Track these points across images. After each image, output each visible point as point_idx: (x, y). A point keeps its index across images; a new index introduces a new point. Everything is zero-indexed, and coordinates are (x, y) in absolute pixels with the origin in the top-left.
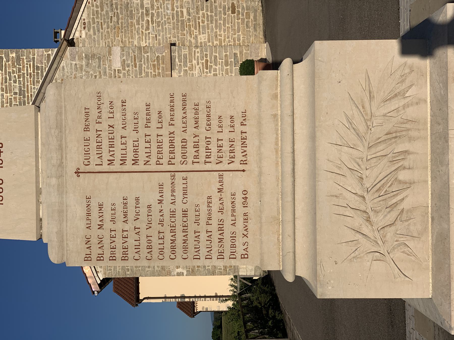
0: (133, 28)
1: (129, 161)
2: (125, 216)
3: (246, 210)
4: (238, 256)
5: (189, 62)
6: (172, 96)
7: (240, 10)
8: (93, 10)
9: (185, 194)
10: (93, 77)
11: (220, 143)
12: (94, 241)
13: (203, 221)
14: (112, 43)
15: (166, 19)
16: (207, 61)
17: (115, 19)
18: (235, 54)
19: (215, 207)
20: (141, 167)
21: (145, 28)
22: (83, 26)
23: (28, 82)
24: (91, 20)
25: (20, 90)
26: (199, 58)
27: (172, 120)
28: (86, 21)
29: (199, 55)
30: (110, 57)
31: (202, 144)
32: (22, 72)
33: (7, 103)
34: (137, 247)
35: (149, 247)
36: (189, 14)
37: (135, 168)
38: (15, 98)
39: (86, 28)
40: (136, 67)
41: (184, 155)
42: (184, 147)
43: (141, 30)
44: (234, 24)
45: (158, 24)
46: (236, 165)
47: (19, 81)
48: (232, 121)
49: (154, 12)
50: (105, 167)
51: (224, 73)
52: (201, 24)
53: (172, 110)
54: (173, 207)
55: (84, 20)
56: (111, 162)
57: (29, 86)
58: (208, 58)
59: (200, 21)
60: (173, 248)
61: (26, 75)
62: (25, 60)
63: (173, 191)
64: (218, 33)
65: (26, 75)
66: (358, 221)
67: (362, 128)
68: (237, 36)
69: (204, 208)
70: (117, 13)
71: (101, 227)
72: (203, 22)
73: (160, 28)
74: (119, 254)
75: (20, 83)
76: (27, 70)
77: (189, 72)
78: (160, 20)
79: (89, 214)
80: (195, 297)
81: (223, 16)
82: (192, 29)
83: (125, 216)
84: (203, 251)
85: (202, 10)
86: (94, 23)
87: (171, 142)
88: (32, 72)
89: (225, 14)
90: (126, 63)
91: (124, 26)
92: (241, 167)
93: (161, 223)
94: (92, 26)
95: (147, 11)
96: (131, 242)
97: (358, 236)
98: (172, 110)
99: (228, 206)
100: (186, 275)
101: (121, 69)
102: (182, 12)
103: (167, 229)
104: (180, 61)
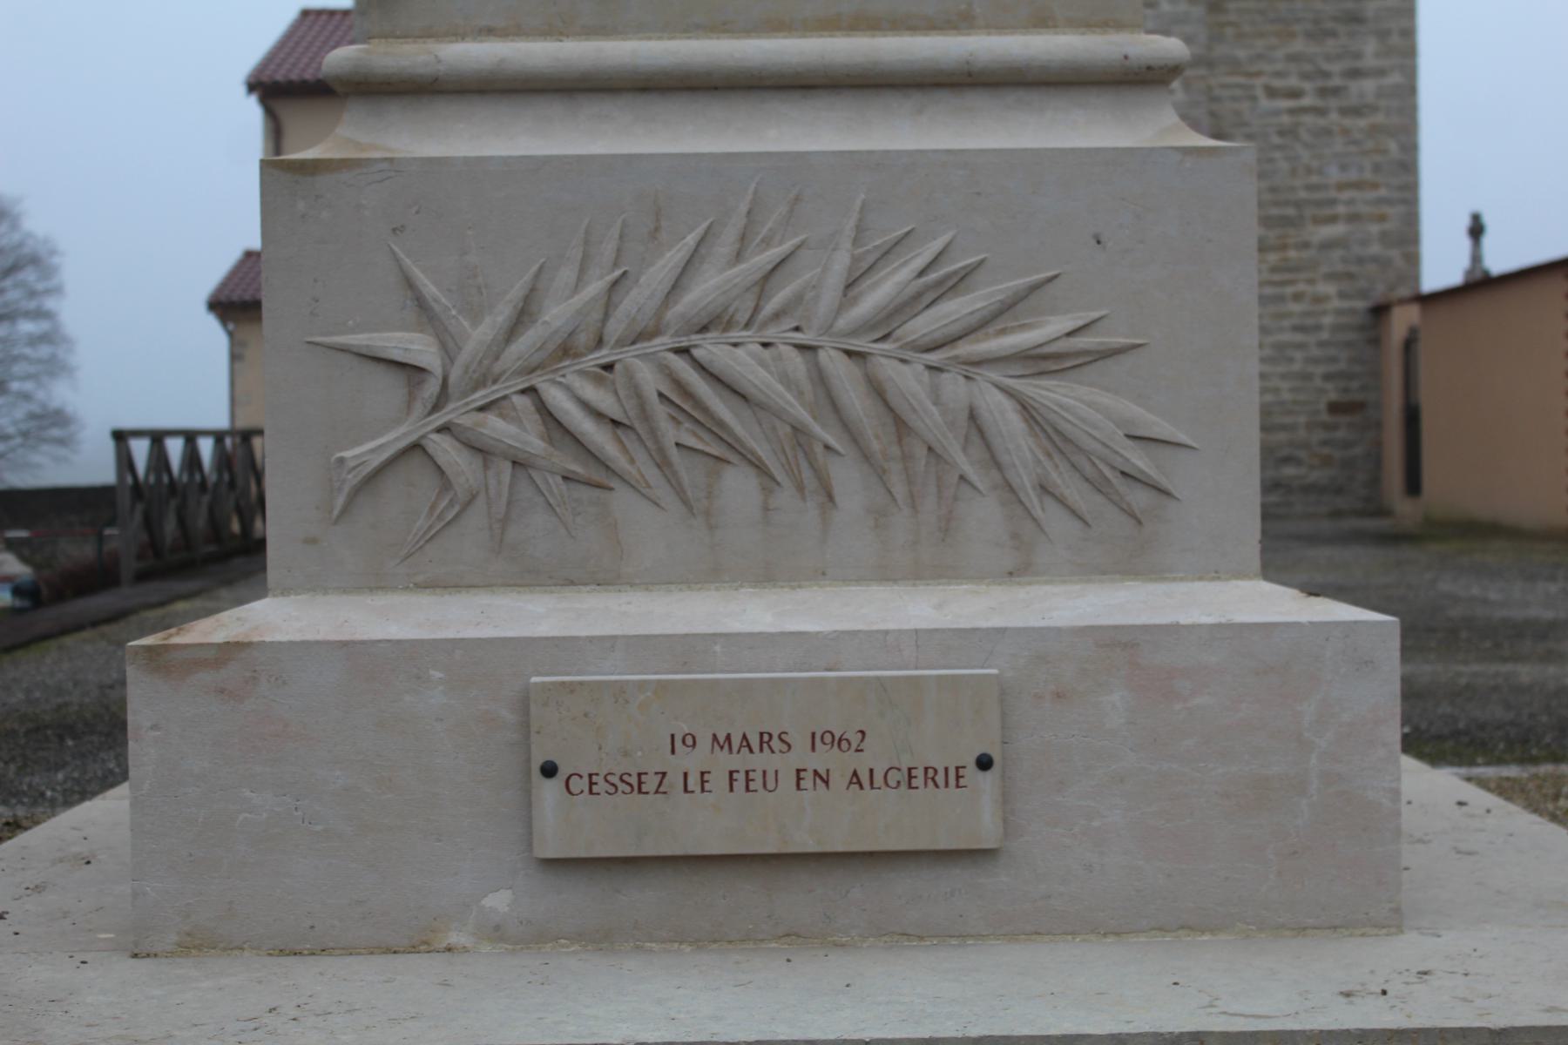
21: (1277, 83)
36: (1327, 245)
52: (1289, 290)
59: (1301, 287)
66: (556, 315)
67: (924, 325)
72: (1297, 297)
73: (1276, 140)
78: (1305, 136)
85: (1342, 295)
89: (1328, 377)
95: (1336, 92)
97: (502, 314)
102: (1333, 219)
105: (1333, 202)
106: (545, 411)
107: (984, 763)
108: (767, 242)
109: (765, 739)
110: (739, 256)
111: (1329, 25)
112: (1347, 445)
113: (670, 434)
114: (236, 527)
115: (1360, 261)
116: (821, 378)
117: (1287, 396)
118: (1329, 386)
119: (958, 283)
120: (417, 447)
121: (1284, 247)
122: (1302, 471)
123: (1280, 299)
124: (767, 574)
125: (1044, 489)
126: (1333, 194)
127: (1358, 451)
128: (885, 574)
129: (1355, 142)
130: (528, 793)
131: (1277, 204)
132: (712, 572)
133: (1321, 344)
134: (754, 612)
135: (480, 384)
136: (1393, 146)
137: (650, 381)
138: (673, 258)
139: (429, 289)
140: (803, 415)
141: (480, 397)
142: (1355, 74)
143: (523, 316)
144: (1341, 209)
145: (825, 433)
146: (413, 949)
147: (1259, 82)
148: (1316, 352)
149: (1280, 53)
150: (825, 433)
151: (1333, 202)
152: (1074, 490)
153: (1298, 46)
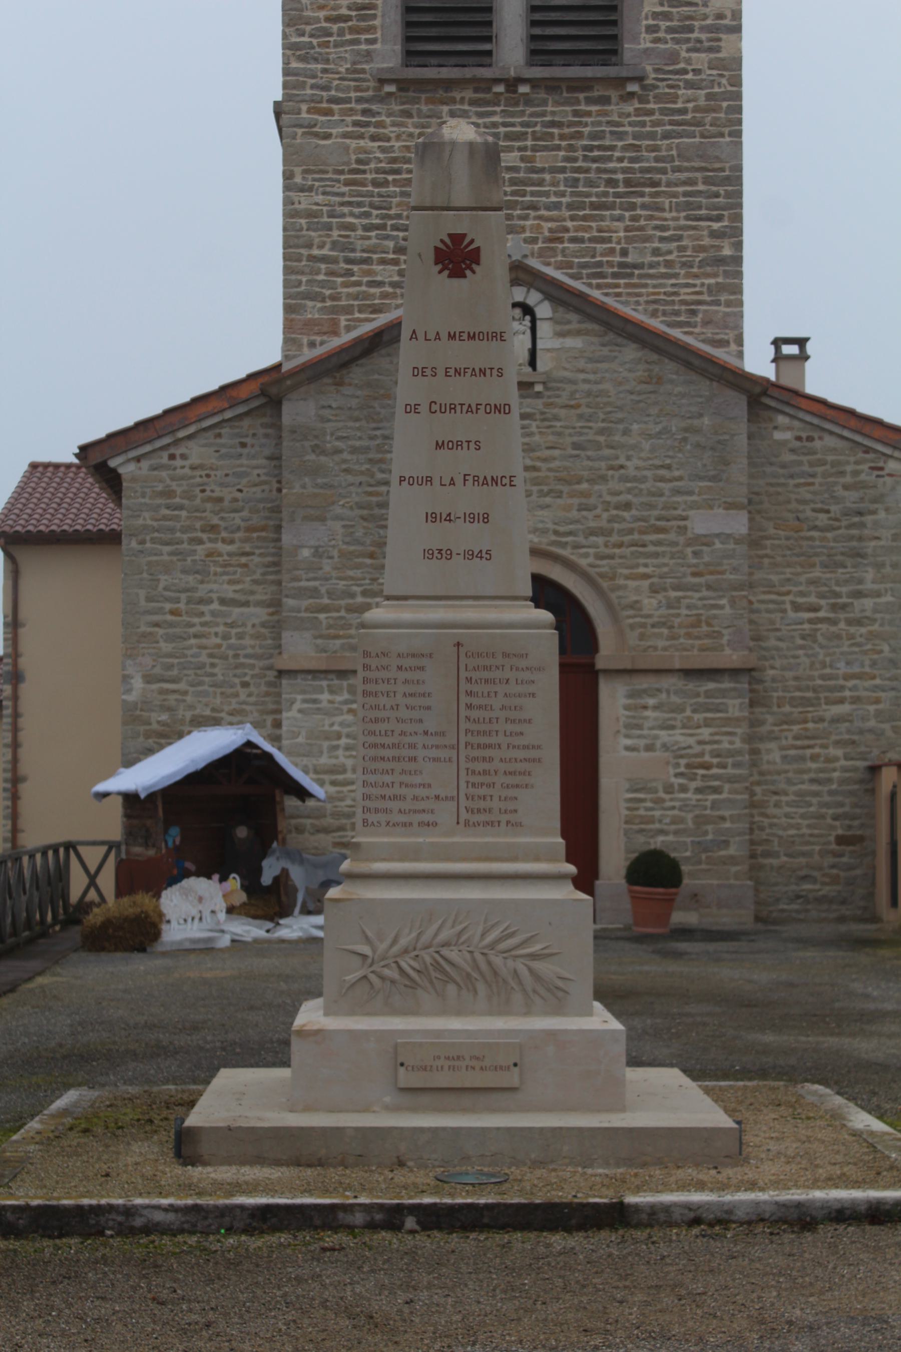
0: (799, 570)
1: (469, 700)
2: (411, 695)
3: (415, 824)
4: (366, 816)
5: (705, 719)
6: (539, 747)
7: (845, 859)
8: (848, 463)
9: (434, 760)
10: (668, 461)
11: (488, 798)
12: (385, 661)
13: (406, 778)
14: (759, 512)
15: (821, 657)
16: (707, 767)
17: (822, 519)
18: (726, 844)
19: (421, 792)
20: (463, 713)
21: (800, 600)
22: (804, 435)
23: (655, 286)
24: (819, 456)
25: (635, 266)
26: (715, 746)
27: (514, 747)
28: (818, 444)
29: (726, 745)
30: (719, 506)
31: (487, 779)
32: (683, 272)
33: (600, 230)
34: (377, 707)
35: (377, 720)
36: (836, 720)
37: (462, 706)
38: (612, 251)
39: (798, 444)
40: (695, 574)
41: (475, 759)
42: (484, 759)
43: (794, 589)
44: (808, 843)
45: (809, 635)
46: (464, 815)
47: (658, 264)
48: (511, 812)
49: (842, 625)
50: (463, 674)
51: (676, 812)
52: (808, 752)
53: (526, 747)
54: (420, 746)
55: (821, 438)
56: (469, 680)
57: (643, 290)
58: (715, 771)
59: (817, 750)
60: (375, 746)
61: (673, 281)
62: (712, 281)
63: (437, 747)
64: (784, 799)
65: (673, 281)
66: (403, 942)
67: (503, 946)
68: (776, 848)
69: (418, 780)
70: (839, 528)
71: (400, 668)
73: (800, 642)
74: (370, 687)
75: (651, 266)
76: (687, 285)
77: (680, 717)
78: (820, 639)
79: (413, 656)
80: (16, 715)
81: (831, 811)
82: (796, 728)
83: (411, 695)
84: (372, 778)
86: (811, 464)
87: (490, 746)
88: (682, 297)
89: (836, 818)
90: (705, 548)
91: (805, 543)
92: (462, 821)
93: (403, 733)
94: (805, 459)
95: (844, 607)
96: (383, 700)
97: (388, 941)
98: (526, 747)
99: (421, 805)
100: (124, 701)
101: (689, 534)
102: (841, 701)
103: (395, 739)
104: (708, 694)
105: (842, 688)
106: (399, 967)
107: (515, 1065)
108: (461, 923)
109: (458, 1058)
110: (453, 927)
111: (839, 558)
112: (850, 868)
113: (434, 974)
114: (38, 916)
115: (861, 732)
116: (474, 960)
117: (805, 831)
118: (837, 823)
119: (512, 935)
120: (365, 977)
121: (805, 721)
122: (817, 887)
123: (802, 759)
124: (459, 1012)
125: (535, 991)
126: (841, 682)
127: (858, 872)
128: (490, 1013)
129: (859, 645)
130: (396, 1070)
131: (799, 689)
132: (443, 1012)
133: (831, 793)
134: (455, 1024)
135: (383, 960)
136: (886, 648)
137: (428, 960)
138: (435, 926)
139: (370, 934)
140: (469, 970)
141: (382, 963)
142: (859, 594)
143: (395, 941)
144: (847, 693)
145: (475, 975)
146: (364, 1111)
147: (787, 598)
148: (827, 798)
149: (802, 579)
150: (475, 975)
151: (842, 688)
152: (542, 991)
153: (817, 573)
